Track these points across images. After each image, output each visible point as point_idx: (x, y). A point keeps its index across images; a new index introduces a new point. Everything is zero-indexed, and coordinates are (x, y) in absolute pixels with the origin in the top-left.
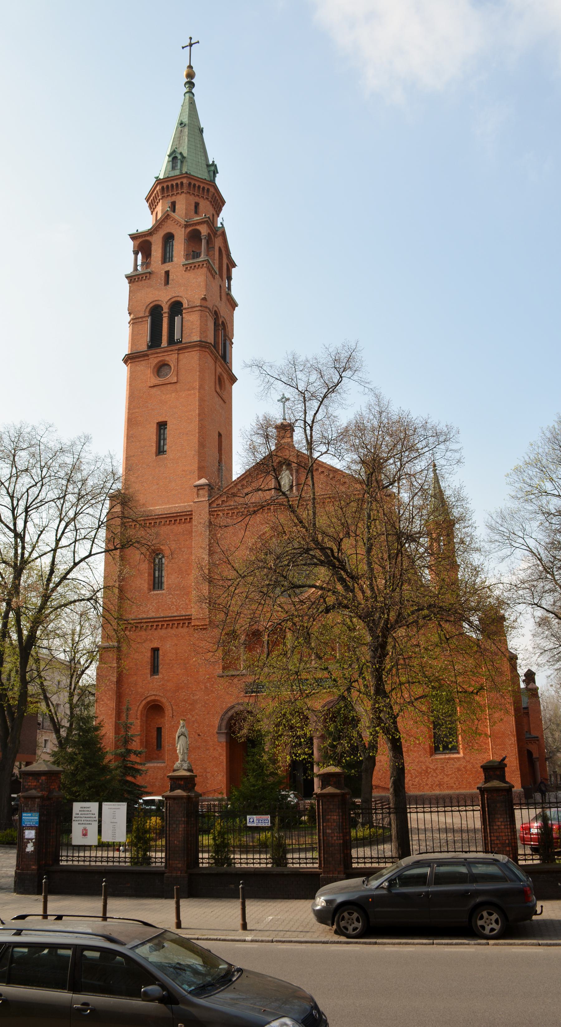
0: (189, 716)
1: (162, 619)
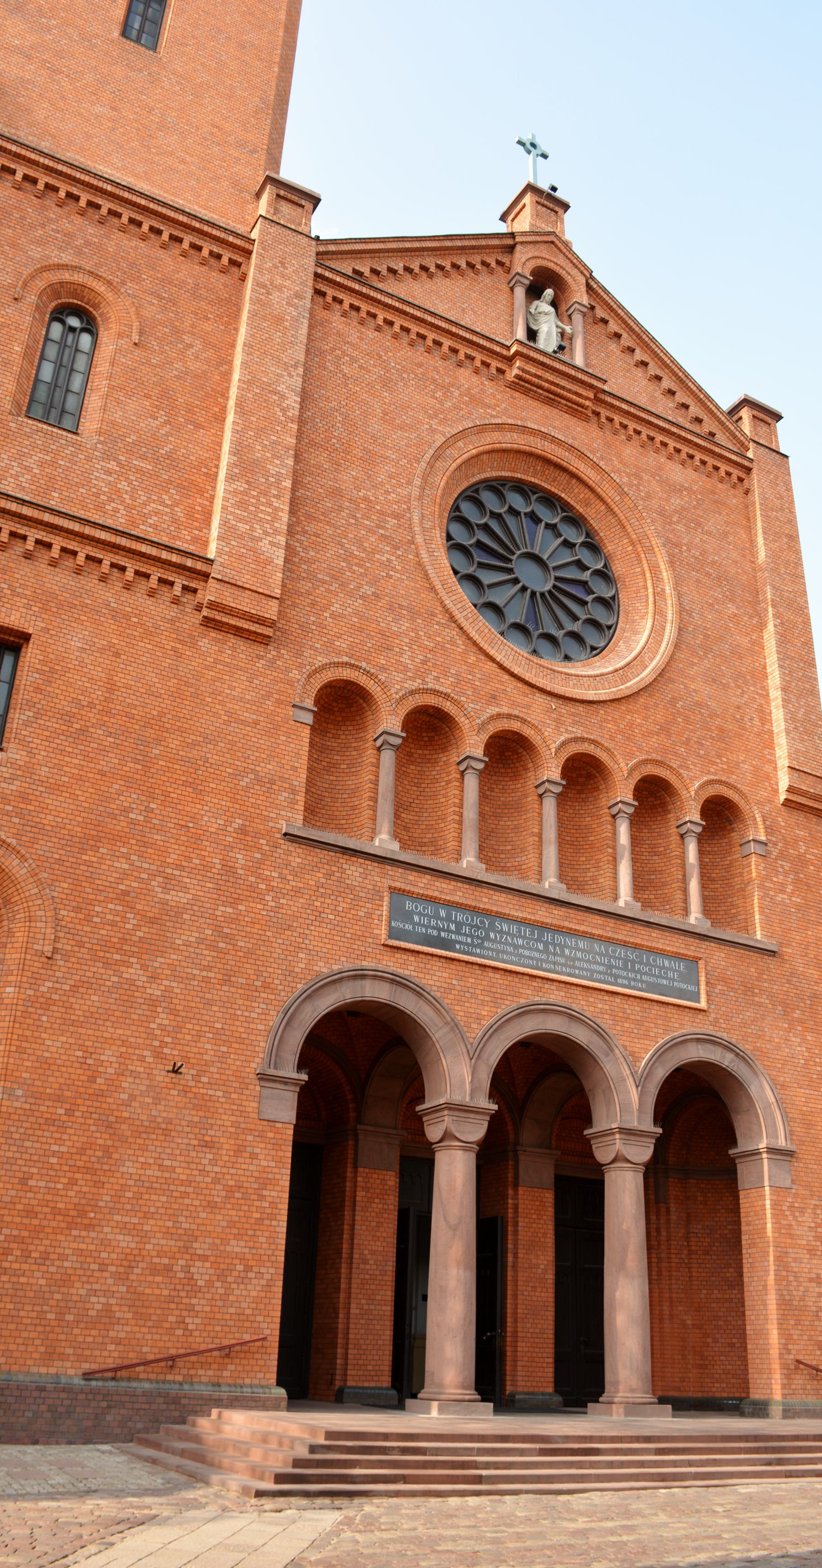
0: (134, 972)
1: (76, 527)
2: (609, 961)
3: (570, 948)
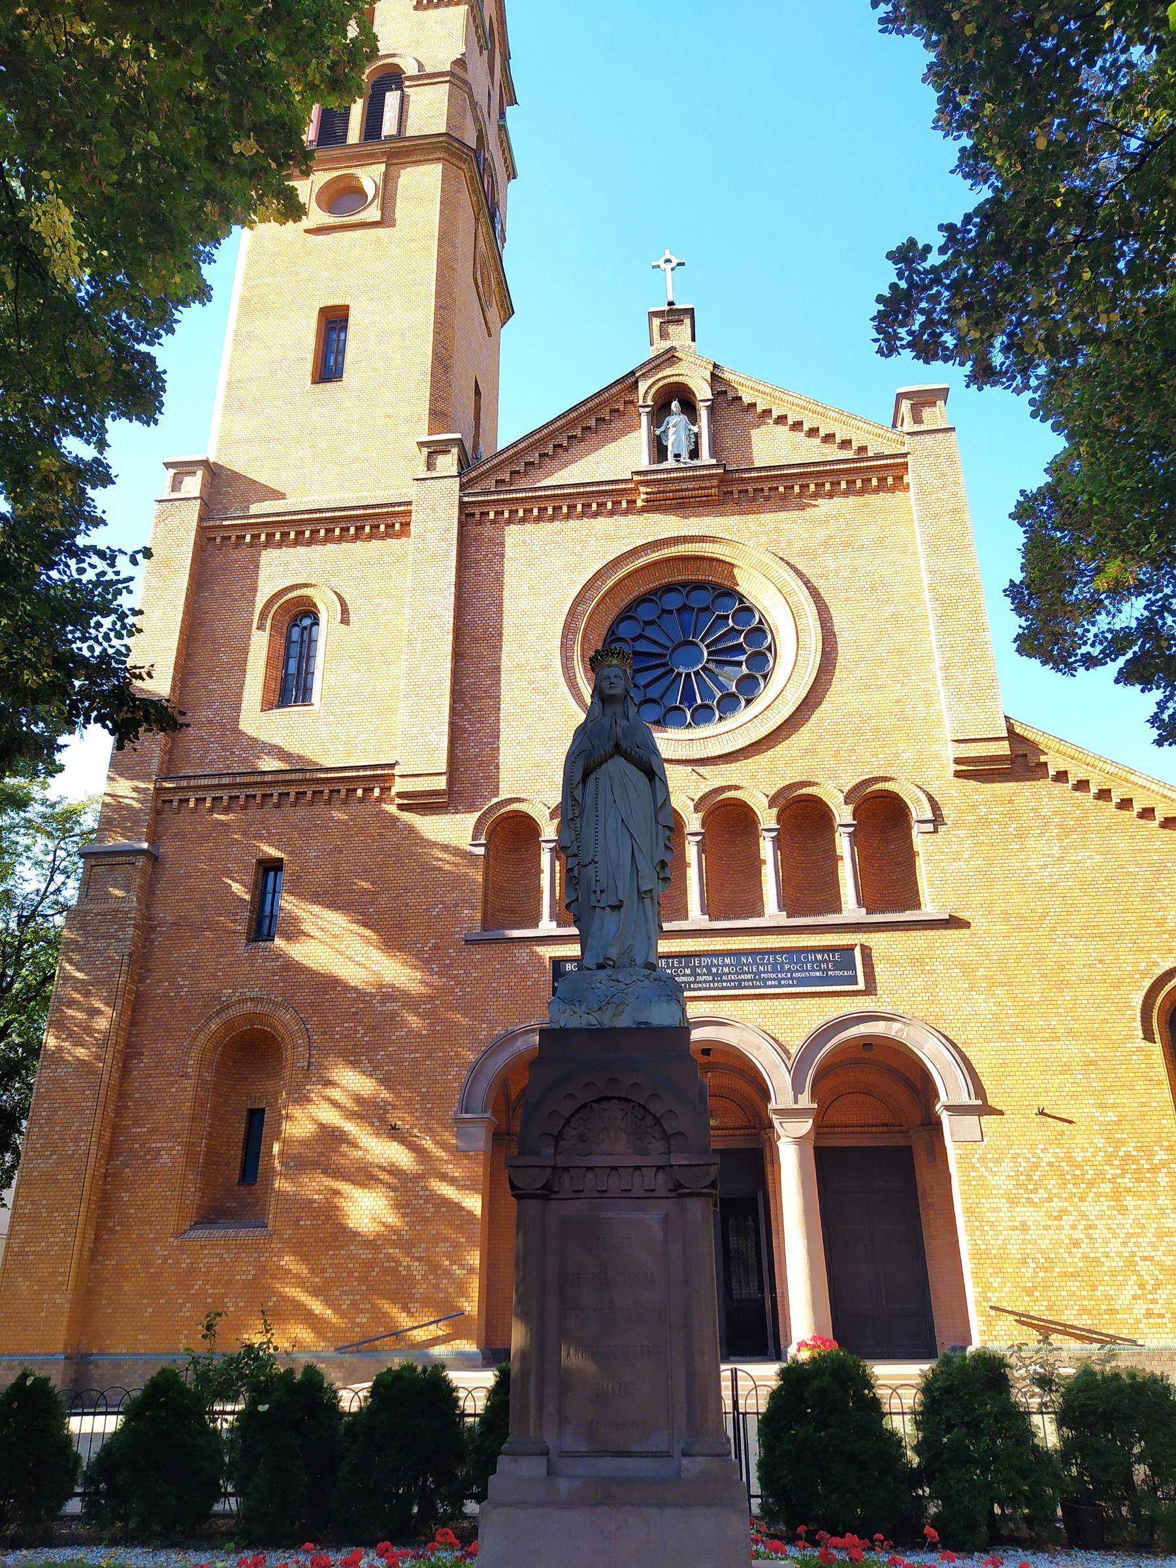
2: (758, 968)
3: (717, 966)
